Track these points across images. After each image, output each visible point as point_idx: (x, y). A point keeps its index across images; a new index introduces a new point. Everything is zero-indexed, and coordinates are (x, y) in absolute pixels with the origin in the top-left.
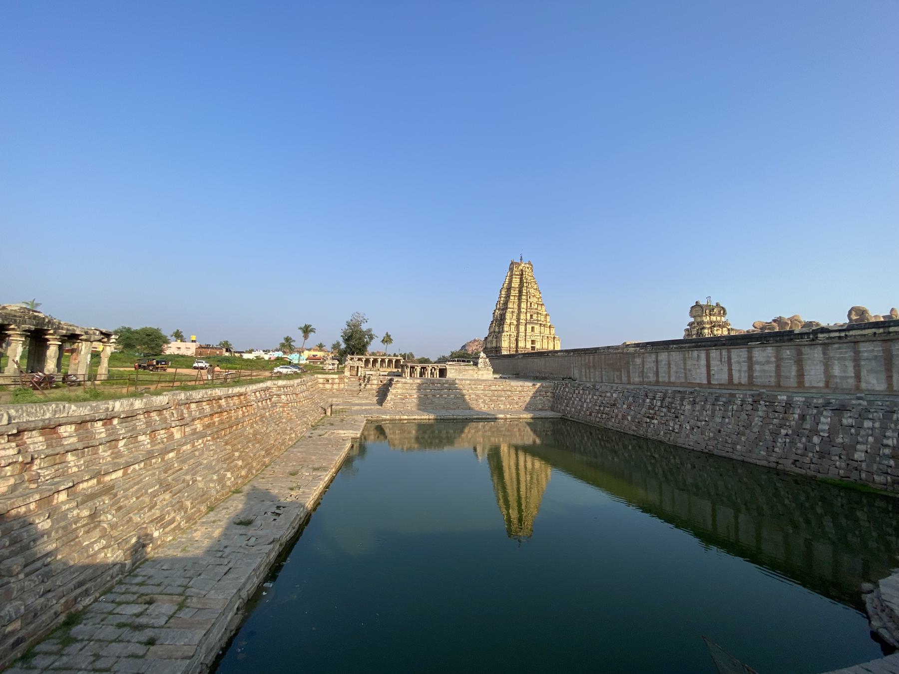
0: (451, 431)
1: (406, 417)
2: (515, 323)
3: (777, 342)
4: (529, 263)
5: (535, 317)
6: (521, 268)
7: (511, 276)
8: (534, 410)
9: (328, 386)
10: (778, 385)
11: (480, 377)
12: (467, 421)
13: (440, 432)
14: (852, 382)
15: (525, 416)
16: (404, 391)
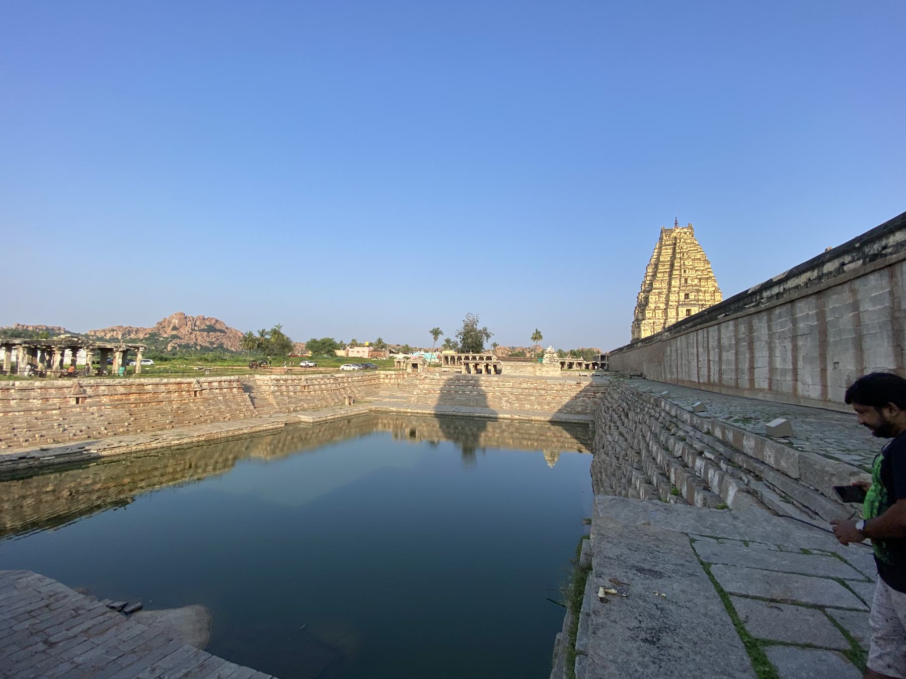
0: (475, 429)
1: (409, 410)
2: (662, 306)
3: (736, 311)
4: (690, 227)
5: (692, 296)
6: (674, 235)
7: (660, 248)
8: (570, 413)
9: (387, 381)
10: (737, 387)
11: (544, 374)
12: (490, 419)
13: (463, 428)
14: (789, 378)
15: (537, 418)
16: (431, 387)
